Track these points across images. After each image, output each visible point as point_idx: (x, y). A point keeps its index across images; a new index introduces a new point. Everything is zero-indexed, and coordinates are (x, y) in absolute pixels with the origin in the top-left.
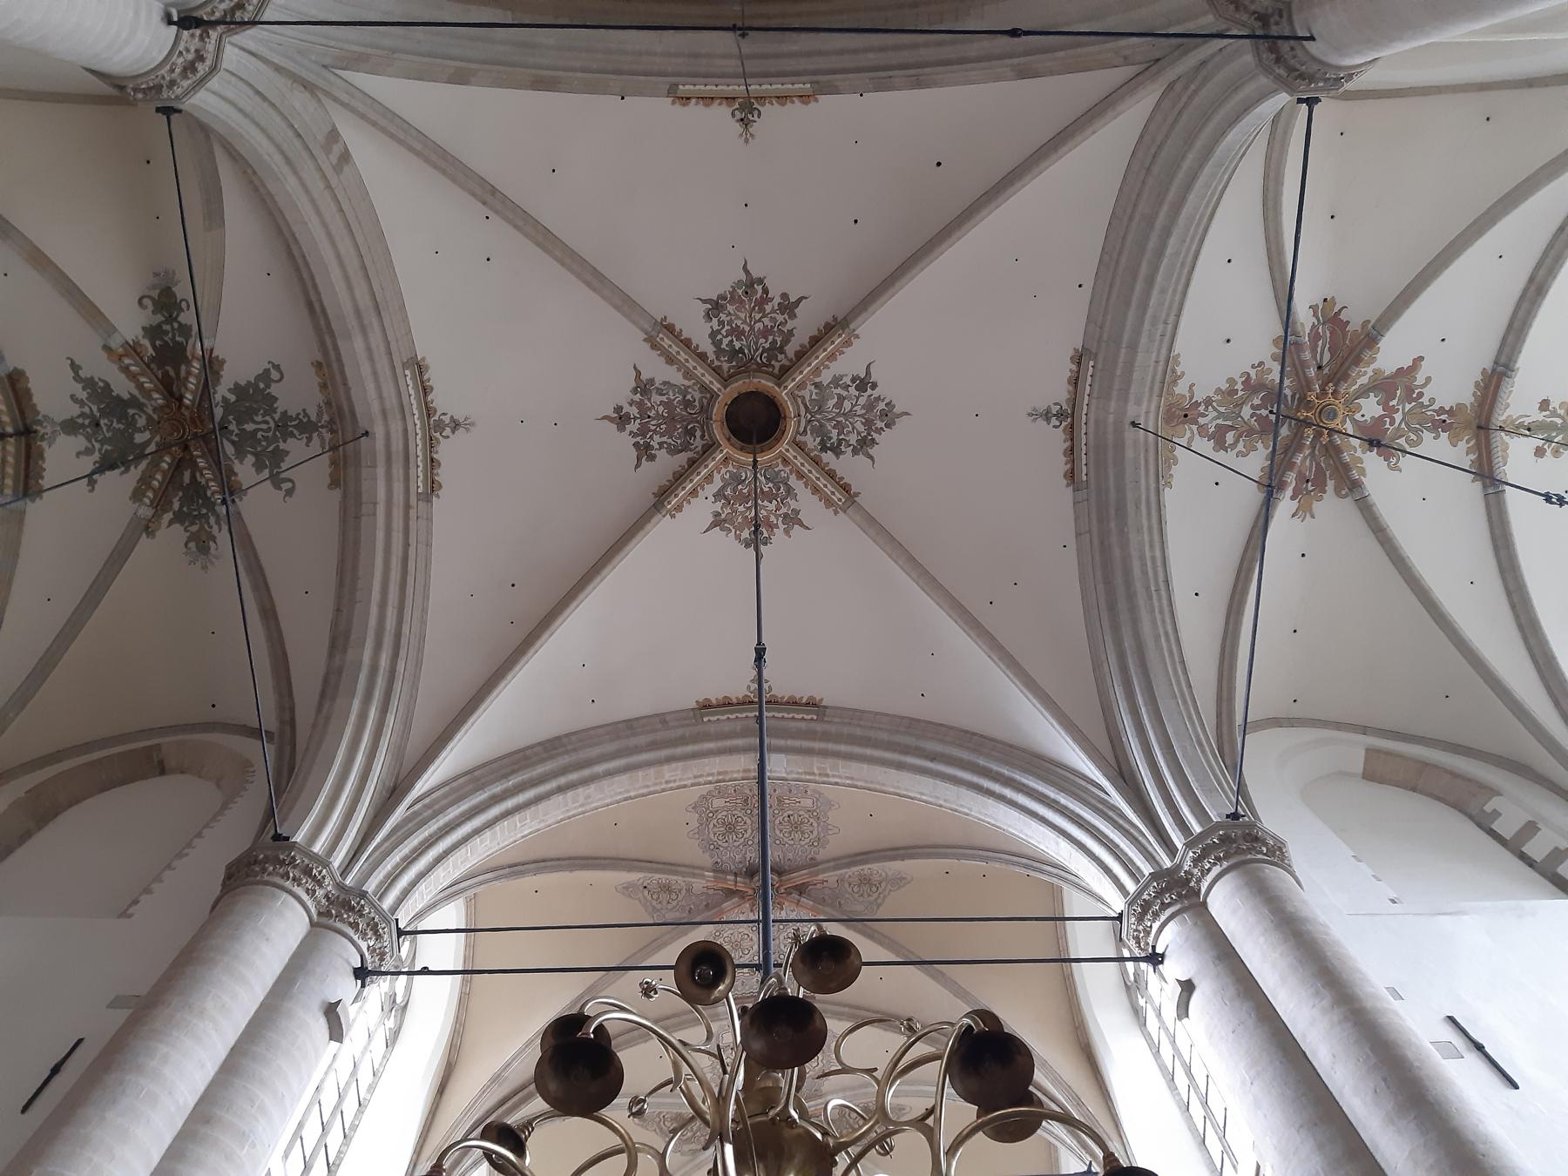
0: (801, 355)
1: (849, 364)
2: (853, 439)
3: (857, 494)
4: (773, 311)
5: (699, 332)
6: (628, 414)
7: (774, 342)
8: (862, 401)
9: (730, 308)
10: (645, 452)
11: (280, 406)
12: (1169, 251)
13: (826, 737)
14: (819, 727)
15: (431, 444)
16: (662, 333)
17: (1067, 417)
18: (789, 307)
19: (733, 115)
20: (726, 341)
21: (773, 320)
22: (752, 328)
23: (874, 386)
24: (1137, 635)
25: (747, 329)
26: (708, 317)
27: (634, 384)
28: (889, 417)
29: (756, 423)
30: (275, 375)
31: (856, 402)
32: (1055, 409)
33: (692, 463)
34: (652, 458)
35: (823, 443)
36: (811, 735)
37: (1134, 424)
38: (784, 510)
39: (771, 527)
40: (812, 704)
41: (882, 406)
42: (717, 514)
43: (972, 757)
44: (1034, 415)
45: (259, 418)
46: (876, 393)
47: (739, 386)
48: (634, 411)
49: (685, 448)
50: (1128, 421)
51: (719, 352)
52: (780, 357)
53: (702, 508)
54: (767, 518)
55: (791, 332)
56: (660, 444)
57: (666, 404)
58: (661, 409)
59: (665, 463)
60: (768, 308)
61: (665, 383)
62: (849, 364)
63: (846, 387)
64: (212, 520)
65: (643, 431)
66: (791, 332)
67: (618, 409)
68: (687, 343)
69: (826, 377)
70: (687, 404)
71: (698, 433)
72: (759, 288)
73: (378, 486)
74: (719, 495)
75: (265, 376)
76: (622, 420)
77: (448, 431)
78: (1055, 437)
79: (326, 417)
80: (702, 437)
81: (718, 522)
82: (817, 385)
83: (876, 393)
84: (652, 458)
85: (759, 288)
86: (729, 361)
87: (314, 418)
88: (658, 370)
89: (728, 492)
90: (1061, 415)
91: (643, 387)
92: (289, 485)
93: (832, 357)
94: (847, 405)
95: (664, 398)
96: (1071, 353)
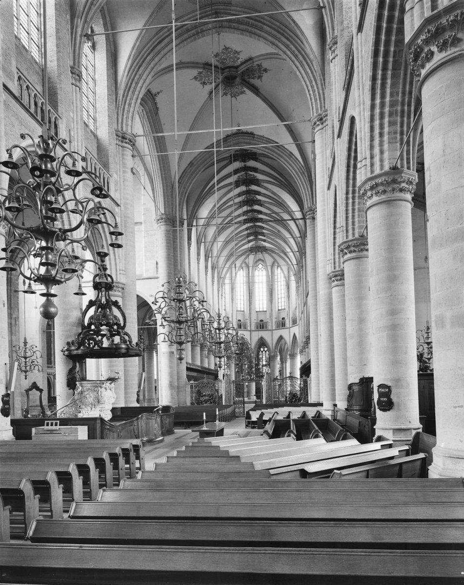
8: (203, 80)
16: (255, 90)
27: (263, 78)
39: (222, 52)
42: (238, 54)
44: (161, 91)
62: (208, 88)
65: (260, 69)
74: (239, 59)
76: (266, 70)
81: (238, 53)
89: (236, 59)
90: (155, 95)
91: (260, 77)
94: (207, 79)
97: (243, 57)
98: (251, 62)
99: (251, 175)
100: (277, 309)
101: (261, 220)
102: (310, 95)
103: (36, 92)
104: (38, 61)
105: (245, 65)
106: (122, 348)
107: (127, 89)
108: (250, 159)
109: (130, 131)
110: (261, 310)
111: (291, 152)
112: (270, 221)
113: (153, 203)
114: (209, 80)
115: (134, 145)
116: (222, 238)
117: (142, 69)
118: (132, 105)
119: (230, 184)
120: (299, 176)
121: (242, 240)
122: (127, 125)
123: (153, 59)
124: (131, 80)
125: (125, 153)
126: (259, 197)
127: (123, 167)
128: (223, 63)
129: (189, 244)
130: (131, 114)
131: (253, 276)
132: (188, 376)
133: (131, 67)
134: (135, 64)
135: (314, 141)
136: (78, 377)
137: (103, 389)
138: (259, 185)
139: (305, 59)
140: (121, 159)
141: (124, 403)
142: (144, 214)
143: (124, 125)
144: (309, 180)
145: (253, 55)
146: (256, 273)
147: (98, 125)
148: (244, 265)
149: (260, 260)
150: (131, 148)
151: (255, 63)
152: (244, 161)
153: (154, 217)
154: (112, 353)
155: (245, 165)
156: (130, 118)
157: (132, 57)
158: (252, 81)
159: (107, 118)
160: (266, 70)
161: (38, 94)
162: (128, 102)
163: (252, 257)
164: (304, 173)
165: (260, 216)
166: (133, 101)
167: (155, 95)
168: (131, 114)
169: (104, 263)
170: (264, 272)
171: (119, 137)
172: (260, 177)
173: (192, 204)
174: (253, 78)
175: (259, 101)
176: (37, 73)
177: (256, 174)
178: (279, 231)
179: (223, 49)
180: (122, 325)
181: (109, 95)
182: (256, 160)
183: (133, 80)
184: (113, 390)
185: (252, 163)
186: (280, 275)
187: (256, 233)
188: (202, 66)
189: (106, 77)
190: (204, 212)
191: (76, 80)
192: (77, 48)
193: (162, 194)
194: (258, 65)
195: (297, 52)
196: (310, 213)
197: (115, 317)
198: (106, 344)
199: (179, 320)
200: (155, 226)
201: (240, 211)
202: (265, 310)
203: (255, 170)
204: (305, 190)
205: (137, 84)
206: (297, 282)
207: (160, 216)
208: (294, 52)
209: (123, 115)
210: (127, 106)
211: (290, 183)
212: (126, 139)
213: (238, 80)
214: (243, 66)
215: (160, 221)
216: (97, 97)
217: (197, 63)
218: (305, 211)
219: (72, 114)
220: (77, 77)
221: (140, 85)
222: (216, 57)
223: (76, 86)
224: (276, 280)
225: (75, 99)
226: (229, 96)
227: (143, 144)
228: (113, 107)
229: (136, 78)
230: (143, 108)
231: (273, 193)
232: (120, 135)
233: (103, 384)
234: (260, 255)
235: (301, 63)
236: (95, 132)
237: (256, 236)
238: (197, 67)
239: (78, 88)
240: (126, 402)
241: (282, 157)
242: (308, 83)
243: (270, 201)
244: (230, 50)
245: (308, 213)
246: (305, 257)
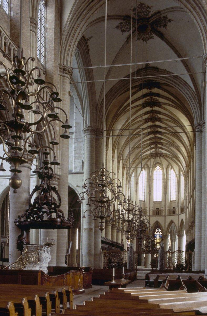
8: (123, 29)
16: (162, 36)
32: (89, 40)
38: (136, 11)
39: (138, 8)
44: (92, 37)
46: (121, 30)
48: (167, 22)
62: (126, 34)
63: (126, 30)
67: (170, 22)
74: (150, 12)
76: (170, 21)
81: (150, 7)
83: (121, 30)
89: (148, 12)
90: (88, 40)
91: (165, 26)
94: (126, 27)
97: (153, 11)
98: (159, 14)
99: (155, 99)
100: (169, 201)
101: (160, 133)
102: (203, 37)
103: (6, 35)
104: (8, 13)
105: (154, 17)
106: (58, 221)
107: (68, 35)
108: (154, 87)
109: (69, 65)
110: (158, 201)
111: (186, 82)
112: (166, 133)
113: (82, 118)
114: (127, 28)
115: (71, 75)
116: (131, 145)
117: (80, 19)
118: (71, 46)
119: (140, 105)
120: (191, 100)
121: (146, 147)
122: (67, 61)
123: (88, 13)
124: (71, 28)
125: (65, 80)
126: (160, 116)
127: (63, 91)
129: (107, 149)
130: (70, 53)
131: (152, 175)
132: (102, 247)
133: (72, 18)
134: (75, 16)
135: (205, 72)
136: (25, 242)
137: (42, 252)
138: (160, 106)
139: (201, 10)
140: (62, 85)
141: (56, 264)
142: (75, 126)
143: (65, 61)
144: (199, 104)
145: (161, 9)
146: (155, 173)
147: (47, 60)
148: (146, 166)
149: (158, 163)
150: (69, 77)
151: (162, 15)
152: (150, 89)
153: (82, 128)
154: (50, 225)
155: (151, 92)
156: (70, 56)
157: (73, 11)
158: (159, 28)
159: (53, 55)
160: (170, 21)
161: (7, 37)
162: (68, 44)
163: (152, 160)
164: (195, 98)
165: (160, 130)
166: (72, 44)
167: (88, 40)
168: (70, 53)
169: (47, 159)
170: (161, 172)
171: (61, 69)
172: (161, 100)
173: (110, 120)
174: (160, 27)
175: (163, 43)
176: (7, 22)
177: (158, 98)
178: (173, 141)
179: (139, 5)
180: (58, 205)
181: (55, 39)
182: (159, 87)
183: (73, 28)
184: (50, 253)
185: (156, 90)
186: (173, 175)
187: (156, 143)
188: (123, 18)
189: (54, 26)
190: (119, 126)
191: (33, 27)
192: (35, 4)
193: (89, 111)
194: (164, 17)
195: (195, 5)
196: (199, 127)
197: (54, 198)
198: (45, 217)
199: (101, 201)
200: (83, 135)
201: (145, 126)
202: (160, 200)
203: (158, 95)
204: (195, 110)
205: (76, 31)
206: (186, 180)
207: (87, 127)
208: (193, 5)
209: (65, 53)
210: (67, 47)
211: (183, 105)
212: (66, 71)
213: (149, 28)
214: (152, 18)
215: (87, 131)
216: (47, 41)
217: (120, 16)
218: (195, 125)
219: (29, 52)
220: (34, 25)
221: (77, 32)
223: (33, 32)
224: (169, 179)
225: (32, 41)
226: (141, 40)
227: (77, 74)
228: (58, 48)
229: (75, 27)
230: (79, 50)
231: (170, 112)
232: (62, 68)
233: (43, 247)
234: (158, 159)
235: (197, 13)
236: (45, 66)
237: (156, 145)
238: (119, 19)
239: (34, 33)
240: (57, 263)
241: (179, 85)
242: (202, 28)
243: (169, 119)
244: (144, 6)
245: (197, 127)
246: (193, 161)
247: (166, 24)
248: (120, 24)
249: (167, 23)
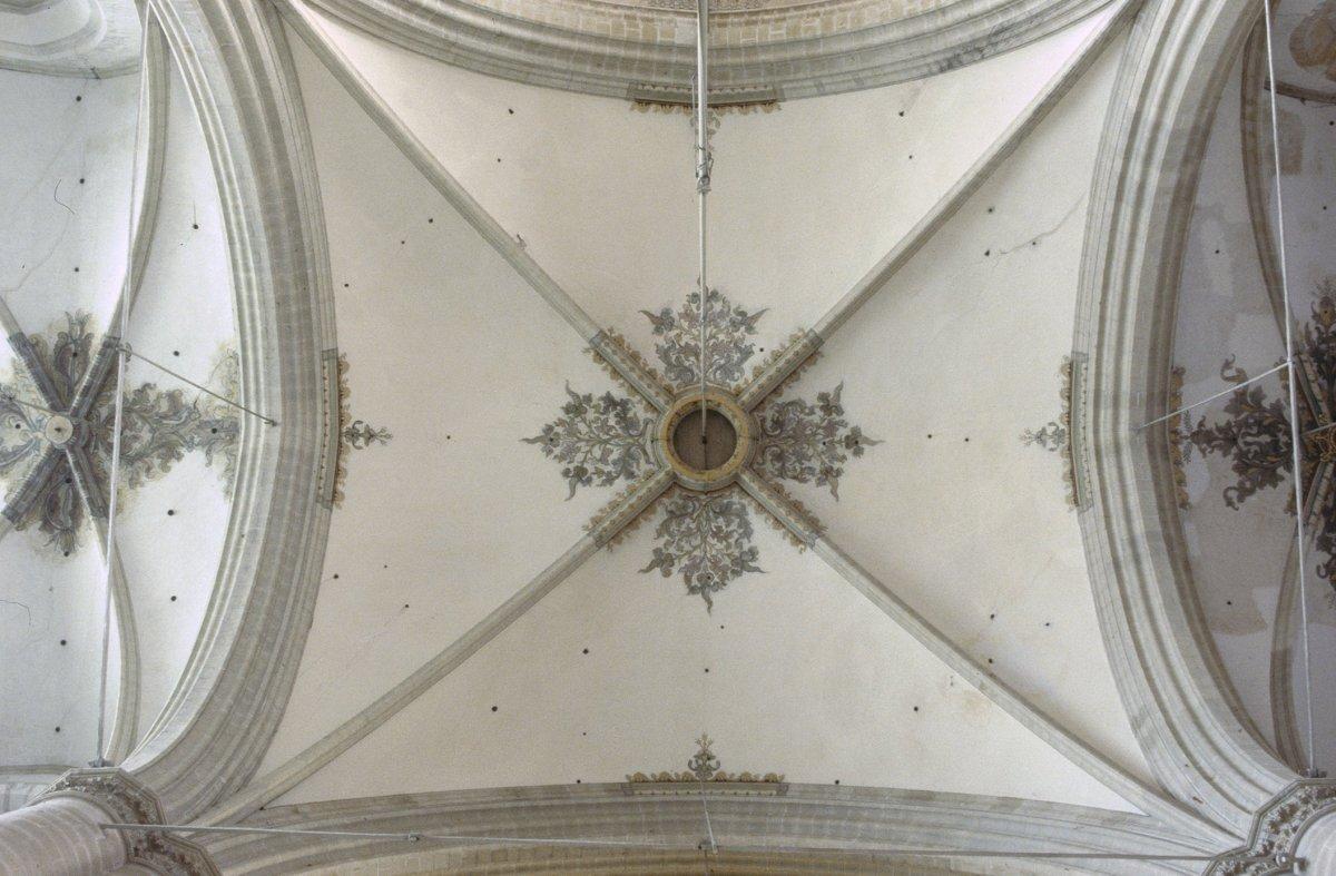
0: (648, 508)
1: (595, 498)
2: (591, 415)
3: (587, 350)
4: (679, 557)
5: (765, 537)
6: (848, 446)
7: (679, 525)
8: (579, 457)
9: (727, 561)
10: (830, 405)
11: (1230, 461)
12: (241, 611)
13: (627, 63)
14: (635, 76)
15: (1070, 417)
17: (345, 435)
18: (662, 561)
19: (718, 763)
20: (733, 527)
21: (680, 548)
22: (704, 540)
23: (566, 473)
24: (264, 181)
25: (710, 539)
26: (753, 553)
27: (841, 480)
28: (548, 438)
29: (699, 431)
30: (1233, 494)
31: (587, 455)
32: (361, 442)
33: (776, 391)
34: (823, 397)
35: (625, 410)
36: (645, 66)
37: (273, 423)
38: (672, 334)
39: (687, 315)
40: (643, 102)
41: (557, 451)
43: (453, 36)
44: (385, 436)
45: (1254, 448)
46: (564, 465)
47: (719, 474)
48: (841, 450)
49: (783, 408)
50: (279, 429)
51: (741, 514)
52: (672, 508)
53: (768, 342)
54: (691, 326)
55: (660, 535)
56: (812, 412)
57: (801, 457)
58: (810, 452)
59: (807, 390)
60: (685, 561)
61: (804, 481)
62: (595, 498)
63: (599, 472)
64: (1315, 336)
65: (831, 428)
66: (660, 535)
67: (858, 452)
68: (778, 523)
69: (621, 484)
70: (780, 457)
71: (769, 424)
72: (695, 582)
73: (1127, 370)
74: (747, 353)
75: (1244, 493)
76: (855, 442)
77: (1050, 430)
78: (360, 409)
79: (1181, 448)
80: (763, 420)
81: (746, 321)
82: (631, 475)
83: (564, 465)
84: (823, 397)
85: (695, 582)
86: (729, 505)
87: (1195, 447)
88: (811, 494)
89: (736, 356)
90: (354, 435)
91: (829, 475)
92: (1229, 373)
93: (614, 505)
94: (597, 452)
95: (807, 464)
96: (344, 504)
128: (683, 371)
158: (790, 485)
160: (855, 442)
188: (593, 333)
222: (658, 331)
244: (718, 307)
247: (836, 465)
248: (567, 410)
249: (844, 458)
